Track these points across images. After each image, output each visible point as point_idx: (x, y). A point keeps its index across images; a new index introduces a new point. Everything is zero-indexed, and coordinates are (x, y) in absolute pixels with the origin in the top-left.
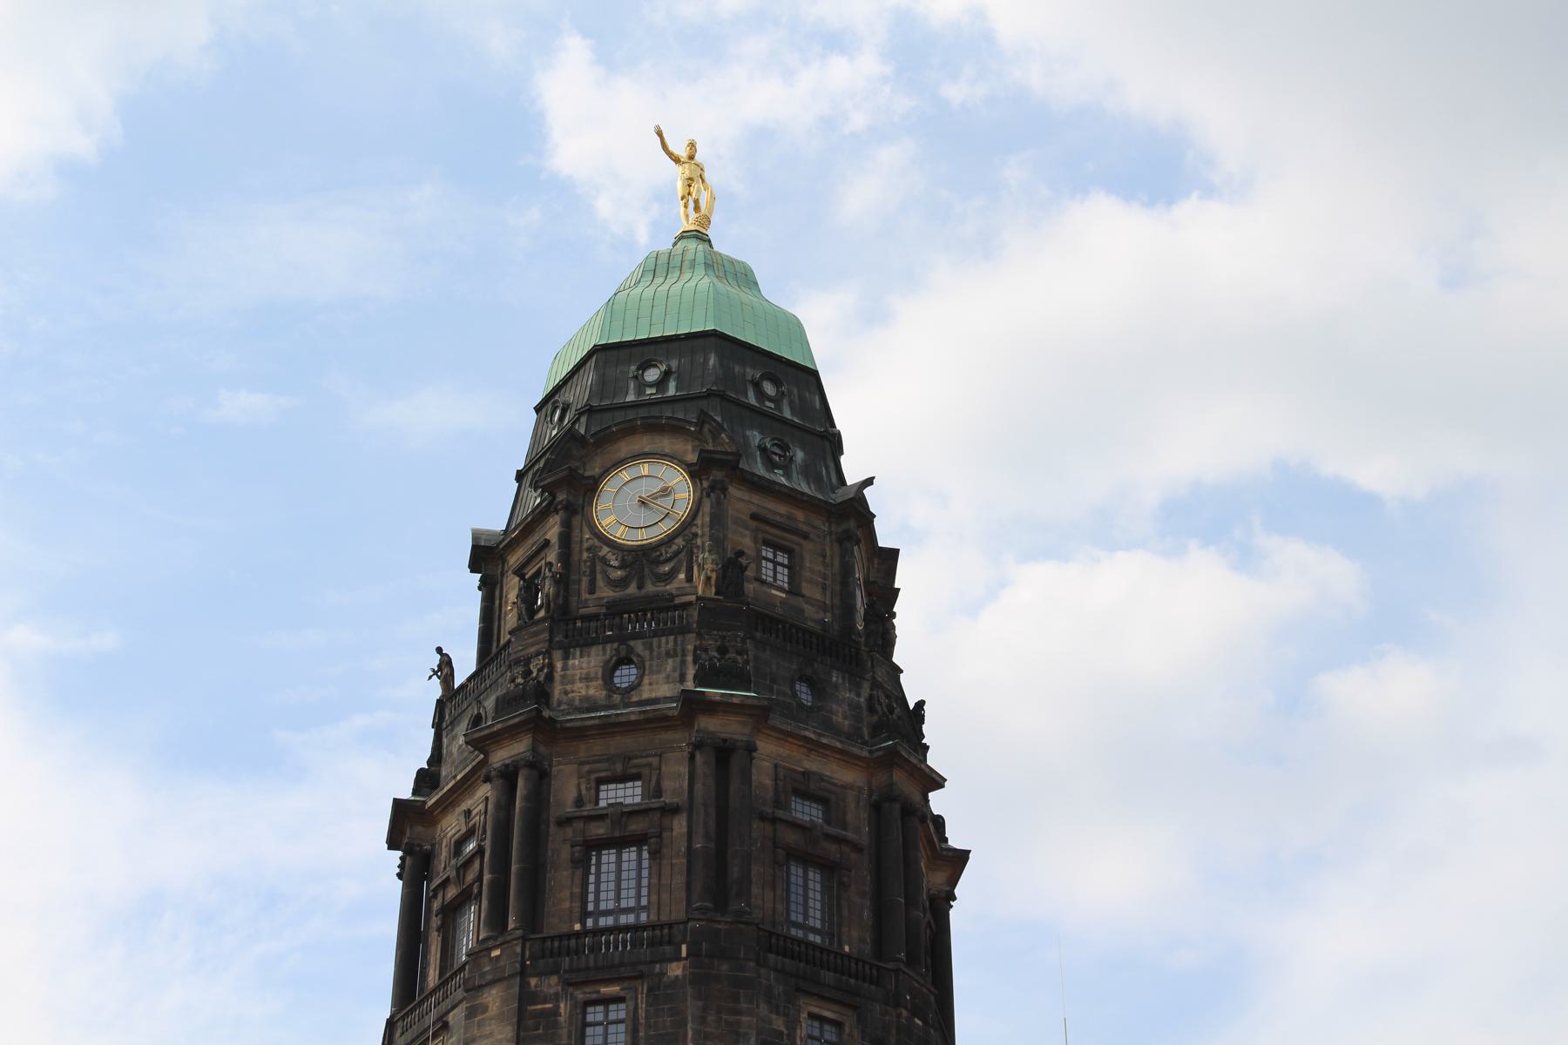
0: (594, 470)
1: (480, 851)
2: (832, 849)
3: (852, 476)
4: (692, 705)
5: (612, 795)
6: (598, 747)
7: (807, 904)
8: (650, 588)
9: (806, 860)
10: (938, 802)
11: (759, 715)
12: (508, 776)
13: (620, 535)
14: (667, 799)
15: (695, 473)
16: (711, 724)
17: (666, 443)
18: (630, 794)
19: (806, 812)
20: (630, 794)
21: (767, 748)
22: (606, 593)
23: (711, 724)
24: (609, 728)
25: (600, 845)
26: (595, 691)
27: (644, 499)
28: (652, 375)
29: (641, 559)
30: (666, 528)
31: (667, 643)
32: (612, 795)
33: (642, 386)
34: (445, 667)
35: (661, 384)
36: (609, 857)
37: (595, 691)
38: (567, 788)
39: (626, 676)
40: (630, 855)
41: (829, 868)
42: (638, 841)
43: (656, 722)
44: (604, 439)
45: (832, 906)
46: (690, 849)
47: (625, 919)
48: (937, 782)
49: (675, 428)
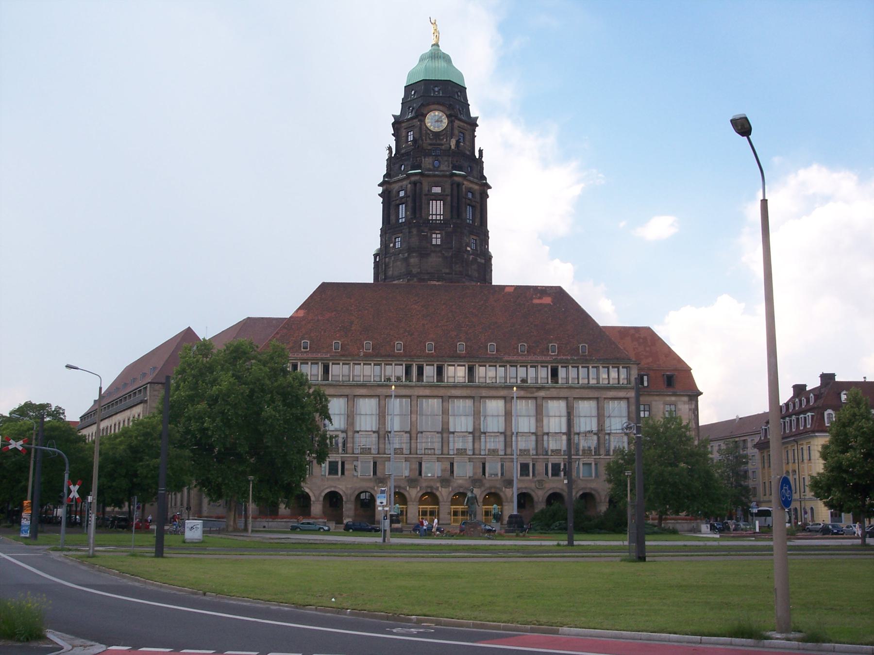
0: (425, 112)
2: (474, 204)
3: (472, 115)
8: (438, 142)
10: (489, 191)
11: (464, 177)
12: (415, 184)
13: (432, 128)
14: (446, 193)
15: (448, 116)
16: (456, 179)
17: (441, 108)
21: (465, 183)
22: (429, 141)
23: (456, 179)
24: (435, 176)
26: (431, 167)
27: (436, 120)
28: (436, 89)
29: (437, 135)
31: (445, 158)
33: (435, 92)
34: (390, 148)
35: (438, 92)
36: (434, 202)
38: (425, 188)
40: (438, 202)
41: (473, 207)
43: (444, 176)
47: (438, 217)
48: (490, 188)
49: (443, 105)
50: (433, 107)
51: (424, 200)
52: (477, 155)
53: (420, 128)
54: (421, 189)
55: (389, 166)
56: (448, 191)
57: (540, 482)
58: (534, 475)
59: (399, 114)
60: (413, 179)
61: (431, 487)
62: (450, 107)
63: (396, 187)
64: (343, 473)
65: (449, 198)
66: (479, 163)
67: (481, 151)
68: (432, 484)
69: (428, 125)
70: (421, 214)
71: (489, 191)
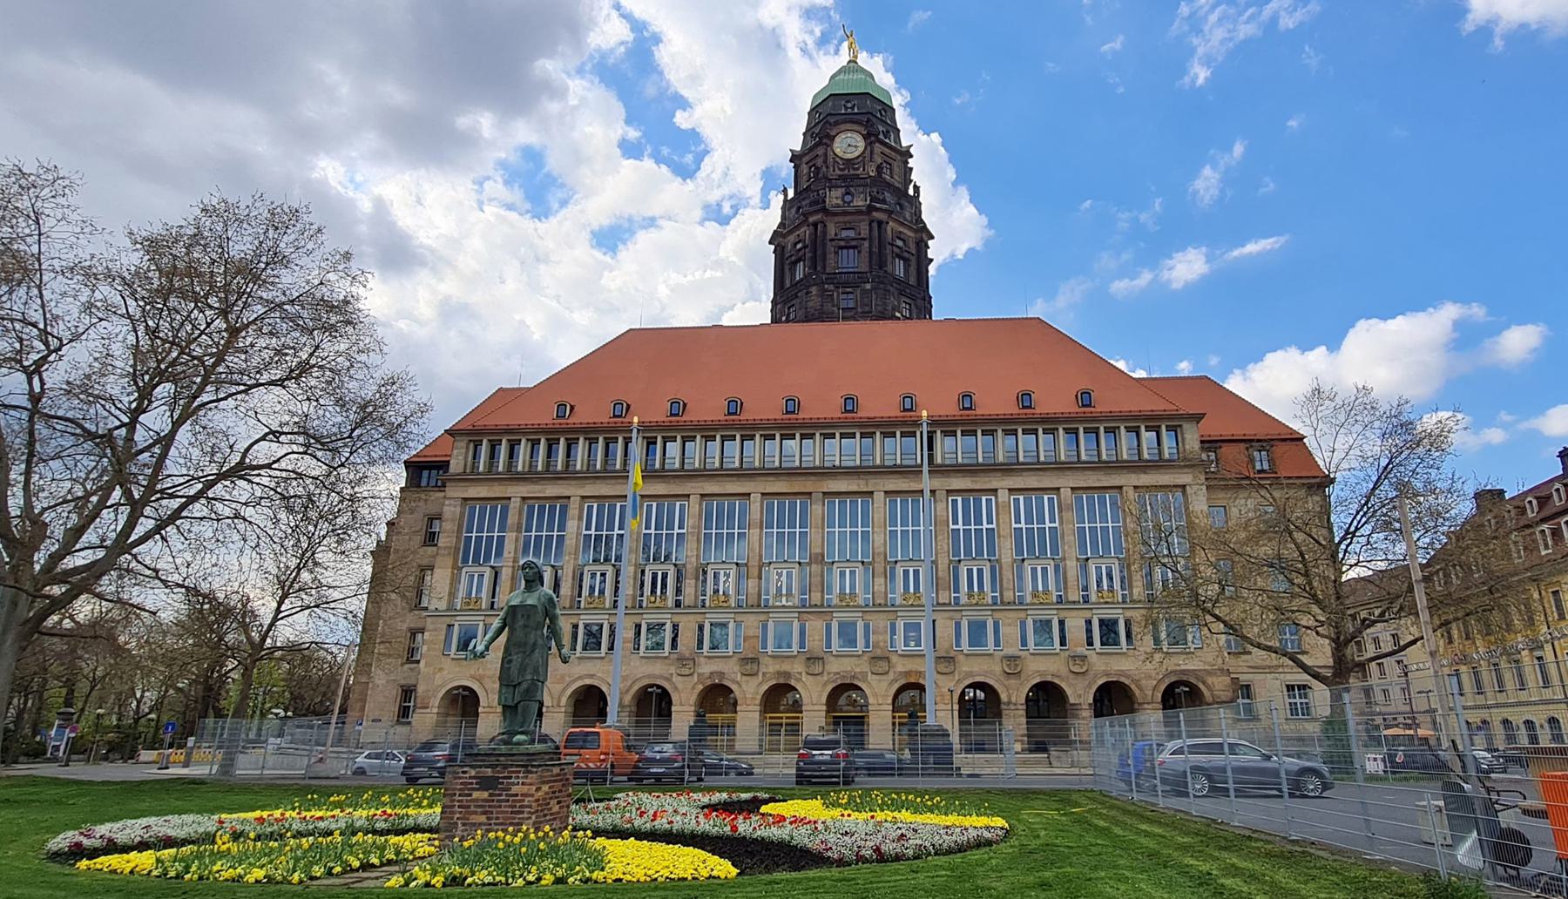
1: (805, 247)
4: (871, 209)
5: (845, 234)
6: (841, 219)
7: (899, 269)
9: (901, 257)
12: (815, 225)
17: (855, 127)
18: (851, 234)
19: (900, 243)
20: (851, 234)
24: (845, 213)
25: (841, 248)
26: (839, 202)
27: (849, 144)
29: (849, 163)
30: (857, 154)
32: (845, 234)
37: (839, 202)
38: (832, 230)
39: (848, 198)
41: (906, 260)
42: (854, 247)
43: (859, 212)
44: (837, 123)
45: (906, 271)
46: (871, 253)
50: (843, 127)
51: (830, 248)
52: (911, 192)
53: (826, 155)
54: (825, 233)
55: (783, 217)
56: (865, 232)
57: (1012, 659)
58: (997, 644)
59: (798, 148)
60: (811, 219)
61: (787, 674)
62: (868, 124)
63: (792, 238)
64: (611, 648)
65: (866, 244)
66: (915, 201)
67: (916, 188)
68: (786, 667)
69: (837, 151)
70: (824, 267)
71: (930, 243)
